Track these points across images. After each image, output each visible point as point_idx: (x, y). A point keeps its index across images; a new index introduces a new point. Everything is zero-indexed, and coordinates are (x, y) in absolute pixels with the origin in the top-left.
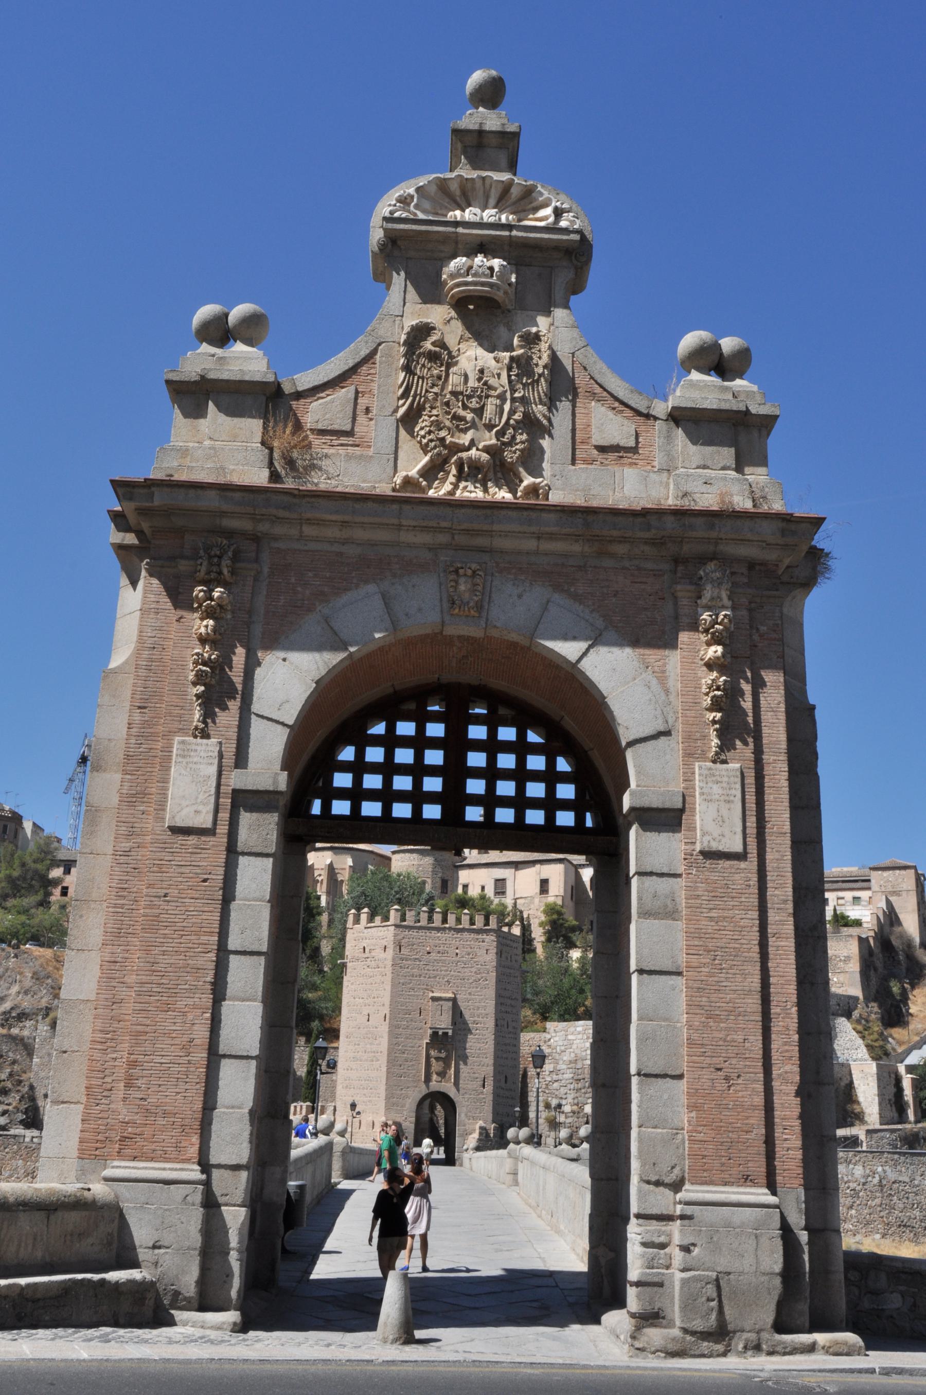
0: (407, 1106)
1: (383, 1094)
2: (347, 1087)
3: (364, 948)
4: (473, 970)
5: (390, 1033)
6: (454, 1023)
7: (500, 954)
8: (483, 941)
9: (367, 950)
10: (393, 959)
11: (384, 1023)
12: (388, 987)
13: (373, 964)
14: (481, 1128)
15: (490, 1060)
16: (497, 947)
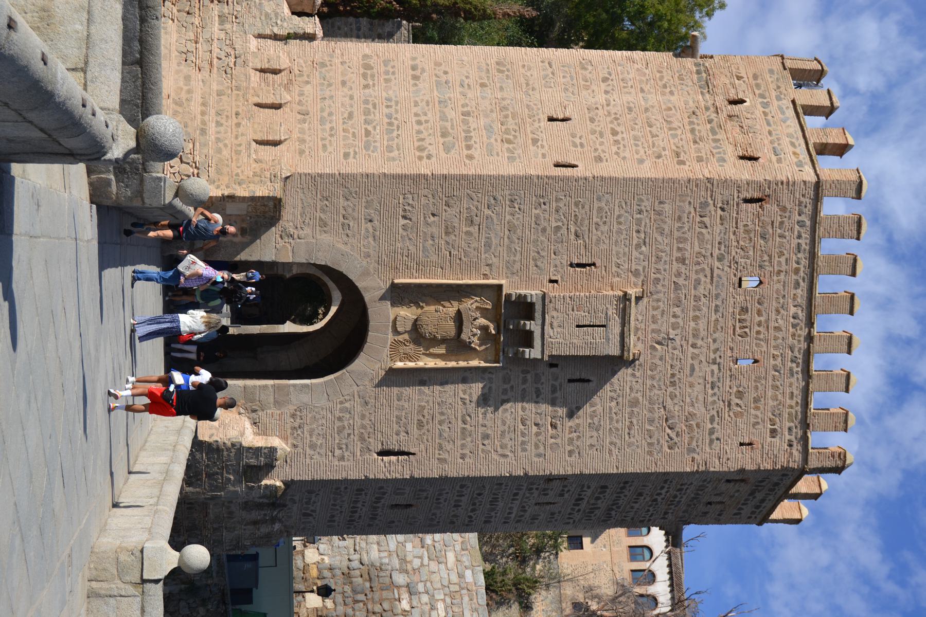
0: (326, 238)
1: (353, 167)
2: (367, 67)
3: (742, 101)
4: (699, 410)
5: (527, 179)
6: (555, 362)
7: (740, 477)
8: (773, 433)
9: (736, 108)
10: (725, 183)
11: (550, 161)
12: (647, 171)
13: (703, 129)
14: (273, 450)
15: (458, 468)
16: (758, 471)
